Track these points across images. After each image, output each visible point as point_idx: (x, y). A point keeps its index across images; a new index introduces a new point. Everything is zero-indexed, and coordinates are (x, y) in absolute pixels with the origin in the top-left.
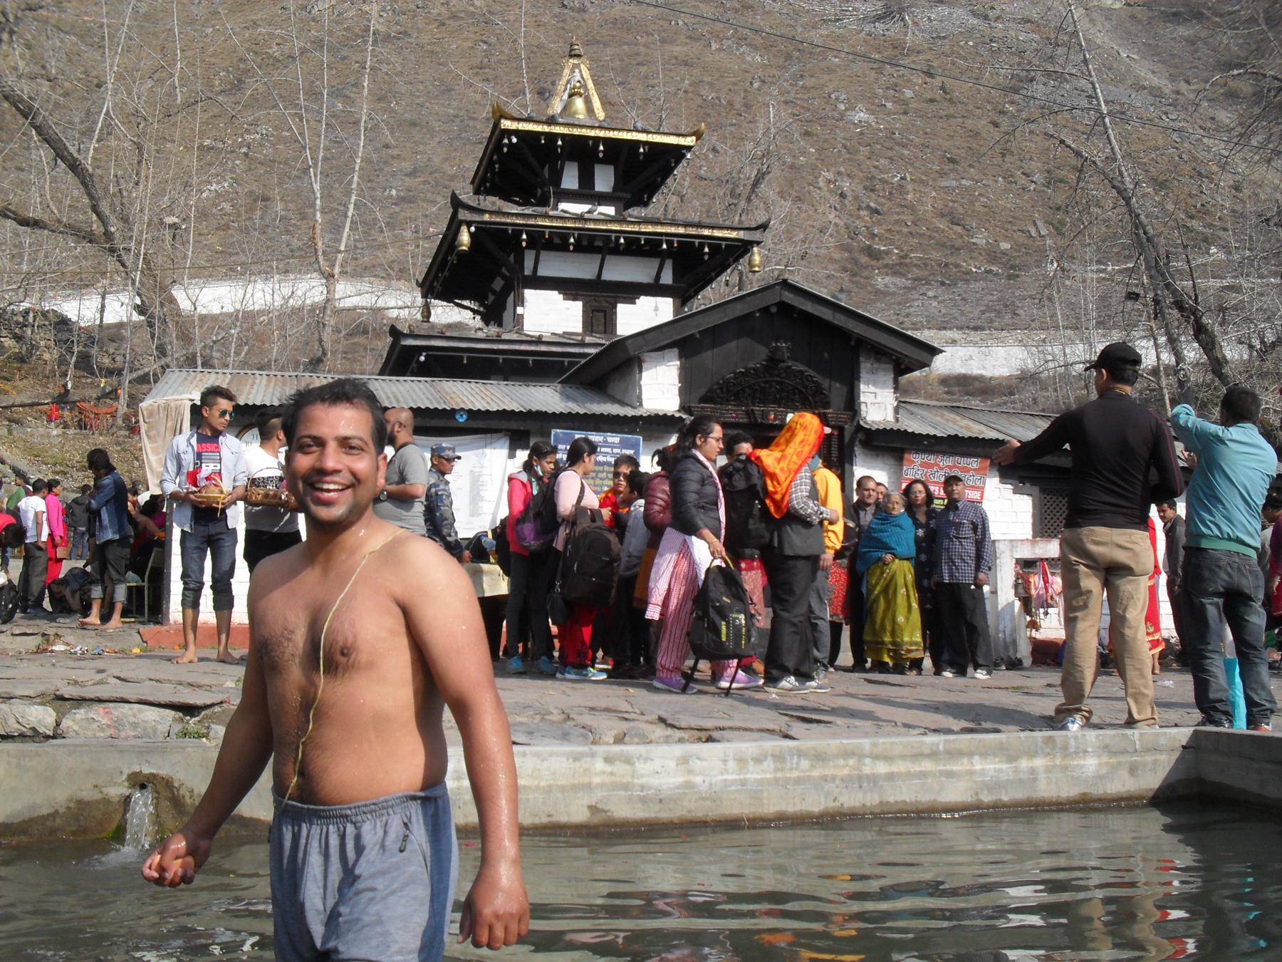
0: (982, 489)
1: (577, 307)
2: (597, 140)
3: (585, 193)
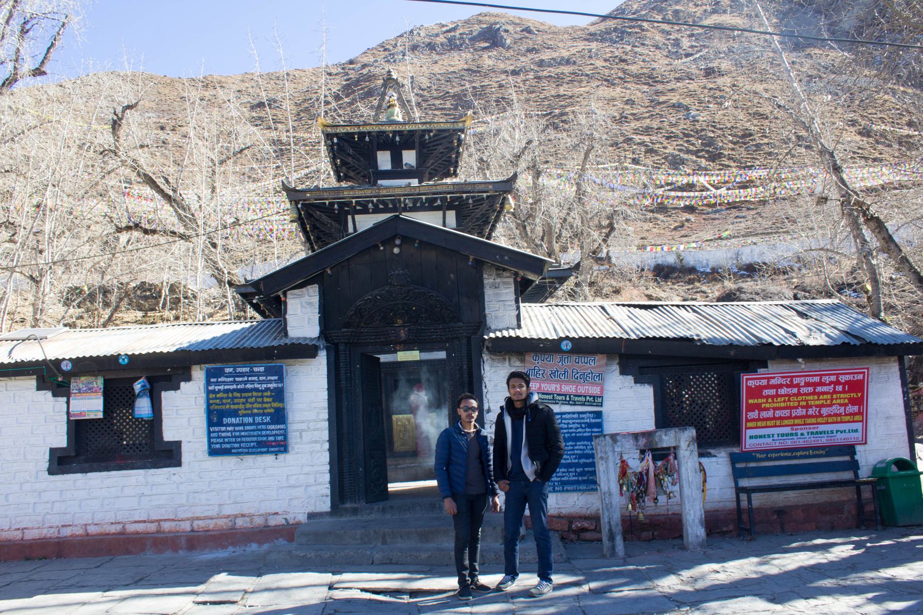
2: (395, 133)
3: (398, 172)
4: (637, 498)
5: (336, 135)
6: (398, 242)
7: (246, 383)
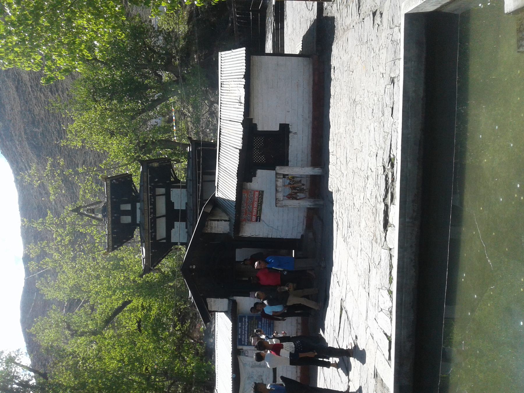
0: (255, 191)
1: (177, 224)
3: (132, 213)
4: (301, 191)
5: (113, 246)
6: (191, 267)
7: (245, 330)
